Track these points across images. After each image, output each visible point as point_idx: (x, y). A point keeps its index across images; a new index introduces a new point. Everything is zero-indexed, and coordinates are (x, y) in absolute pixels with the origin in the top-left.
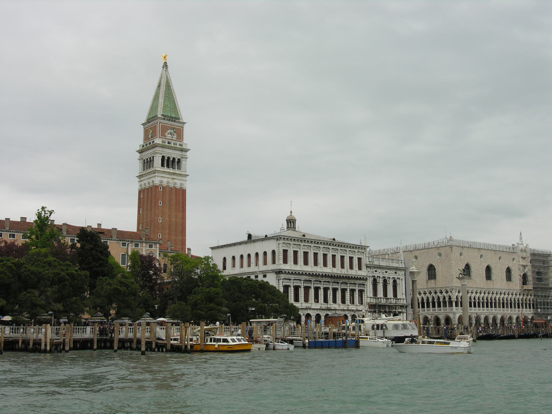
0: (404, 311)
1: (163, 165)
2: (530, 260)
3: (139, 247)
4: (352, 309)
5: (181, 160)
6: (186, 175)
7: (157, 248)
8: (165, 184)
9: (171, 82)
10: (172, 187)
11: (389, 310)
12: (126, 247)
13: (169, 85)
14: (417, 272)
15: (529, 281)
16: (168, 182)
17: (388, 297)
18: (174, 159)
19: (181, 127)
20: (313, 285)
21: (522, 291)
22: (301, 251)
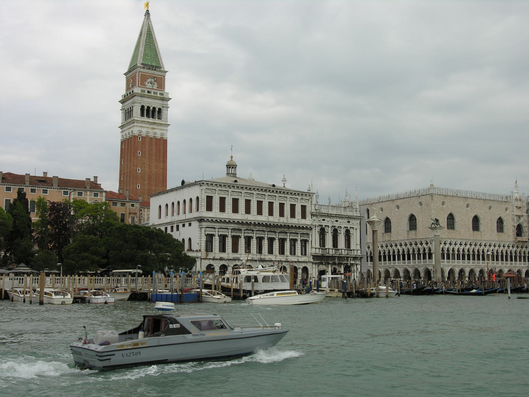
0: (358, 262)
1: (142, 115)
2: (527, 210)
4: (292, 260)
7: (102, 196)
8: (144, 134)
11: (339, 262)
12: (68, 196)
13: (150, 33)
14: (377, 221)
16: (148, 132)
17: (339, 248)
18: (154, 108)
19: (163, 76)
20: (243, 234)
22: (229, 197)
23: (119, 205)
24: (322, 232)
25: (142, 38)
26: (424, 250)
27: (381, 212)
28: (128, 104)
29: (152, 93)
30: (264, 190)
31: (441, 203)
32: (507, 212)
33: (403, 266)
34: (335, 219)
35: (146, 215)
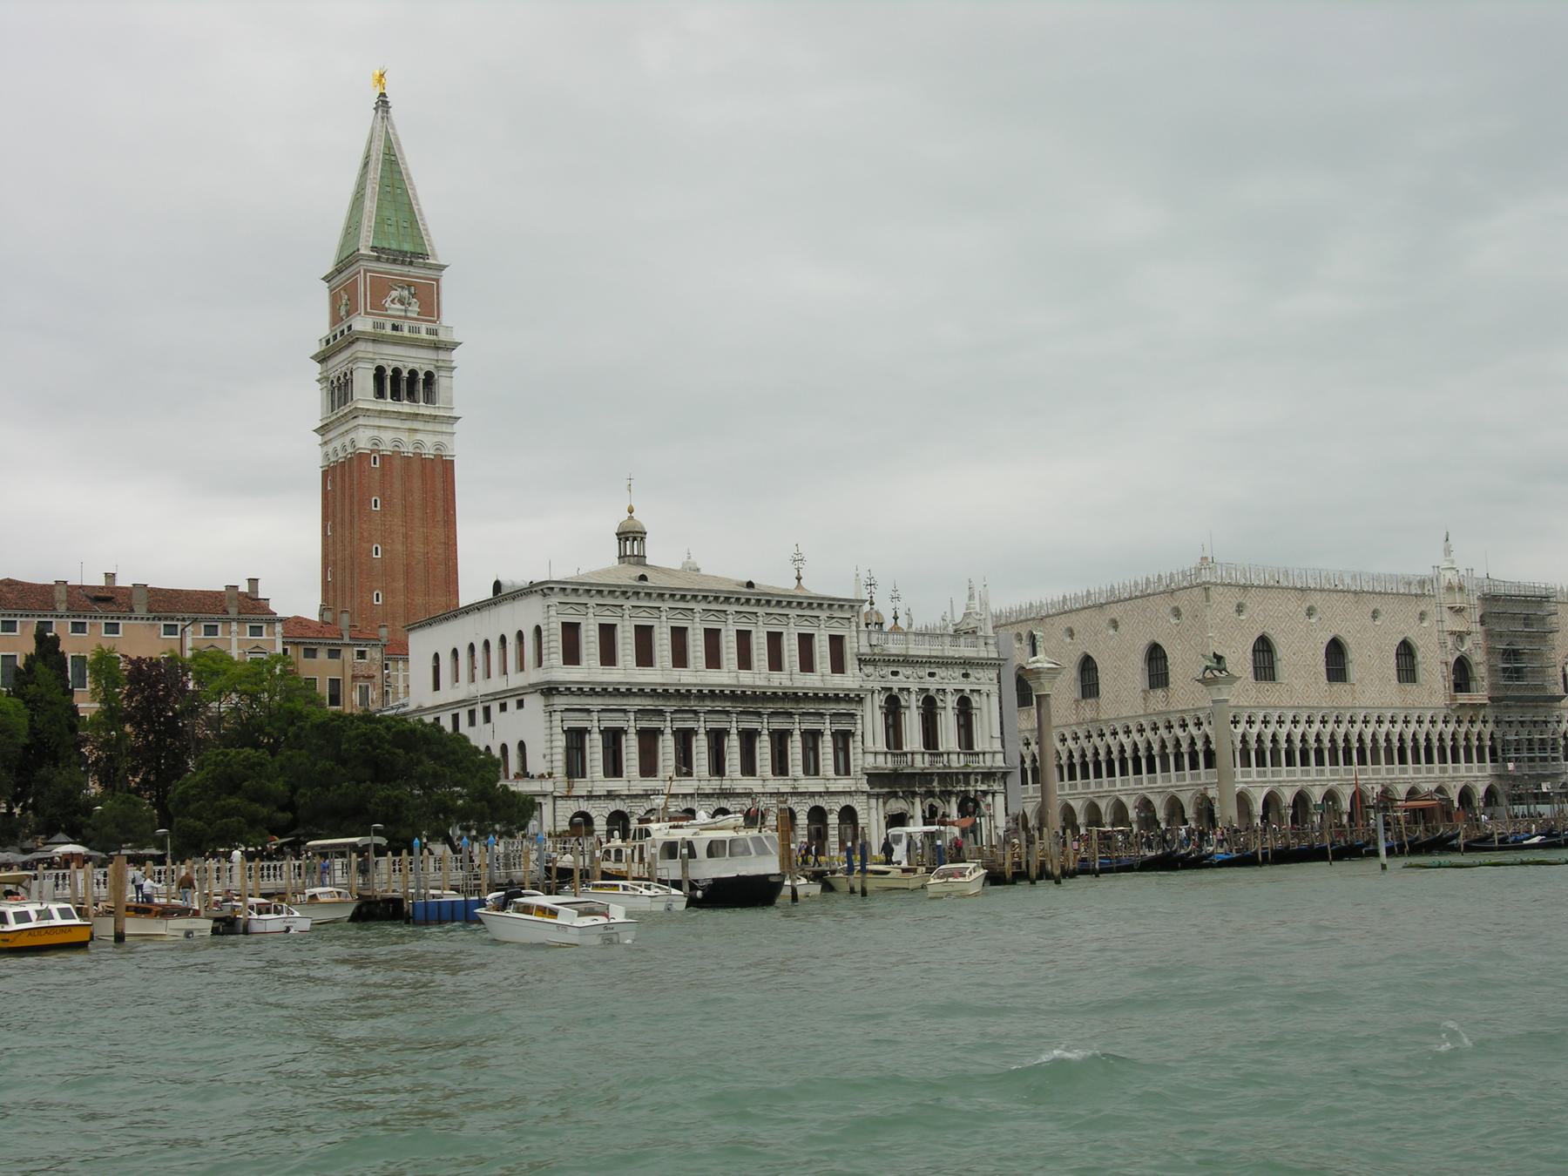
0: (996, 787)
1: (380, 393)
2: (1481, 617)
3: (220, 635)
4: (810, 790)
5: (436, 376)
6: (450, 417)
7: (274, 634)
8: (387, 448)
9: (400, 149)
10: (410, 455)
11: (943, 789)
12: (179, 636)
13: (393, 158)
15: (1476, 680)
17: (941, 749)
18: (413, 373)
19: (434, 280)
20: (669, 724)
21: (1452, 709)
23: (322, 655)
24: (893, 708)
25: (371, 175)
26: (1193, 743)
27: (1068, 640)
28: (338, 363)
29: (406, 329)
30: (722, 599)
31: (1234, 609)
32: (1425, 624)
33: (1135, 789)
34: (928, 670)
35: (401, 679)
